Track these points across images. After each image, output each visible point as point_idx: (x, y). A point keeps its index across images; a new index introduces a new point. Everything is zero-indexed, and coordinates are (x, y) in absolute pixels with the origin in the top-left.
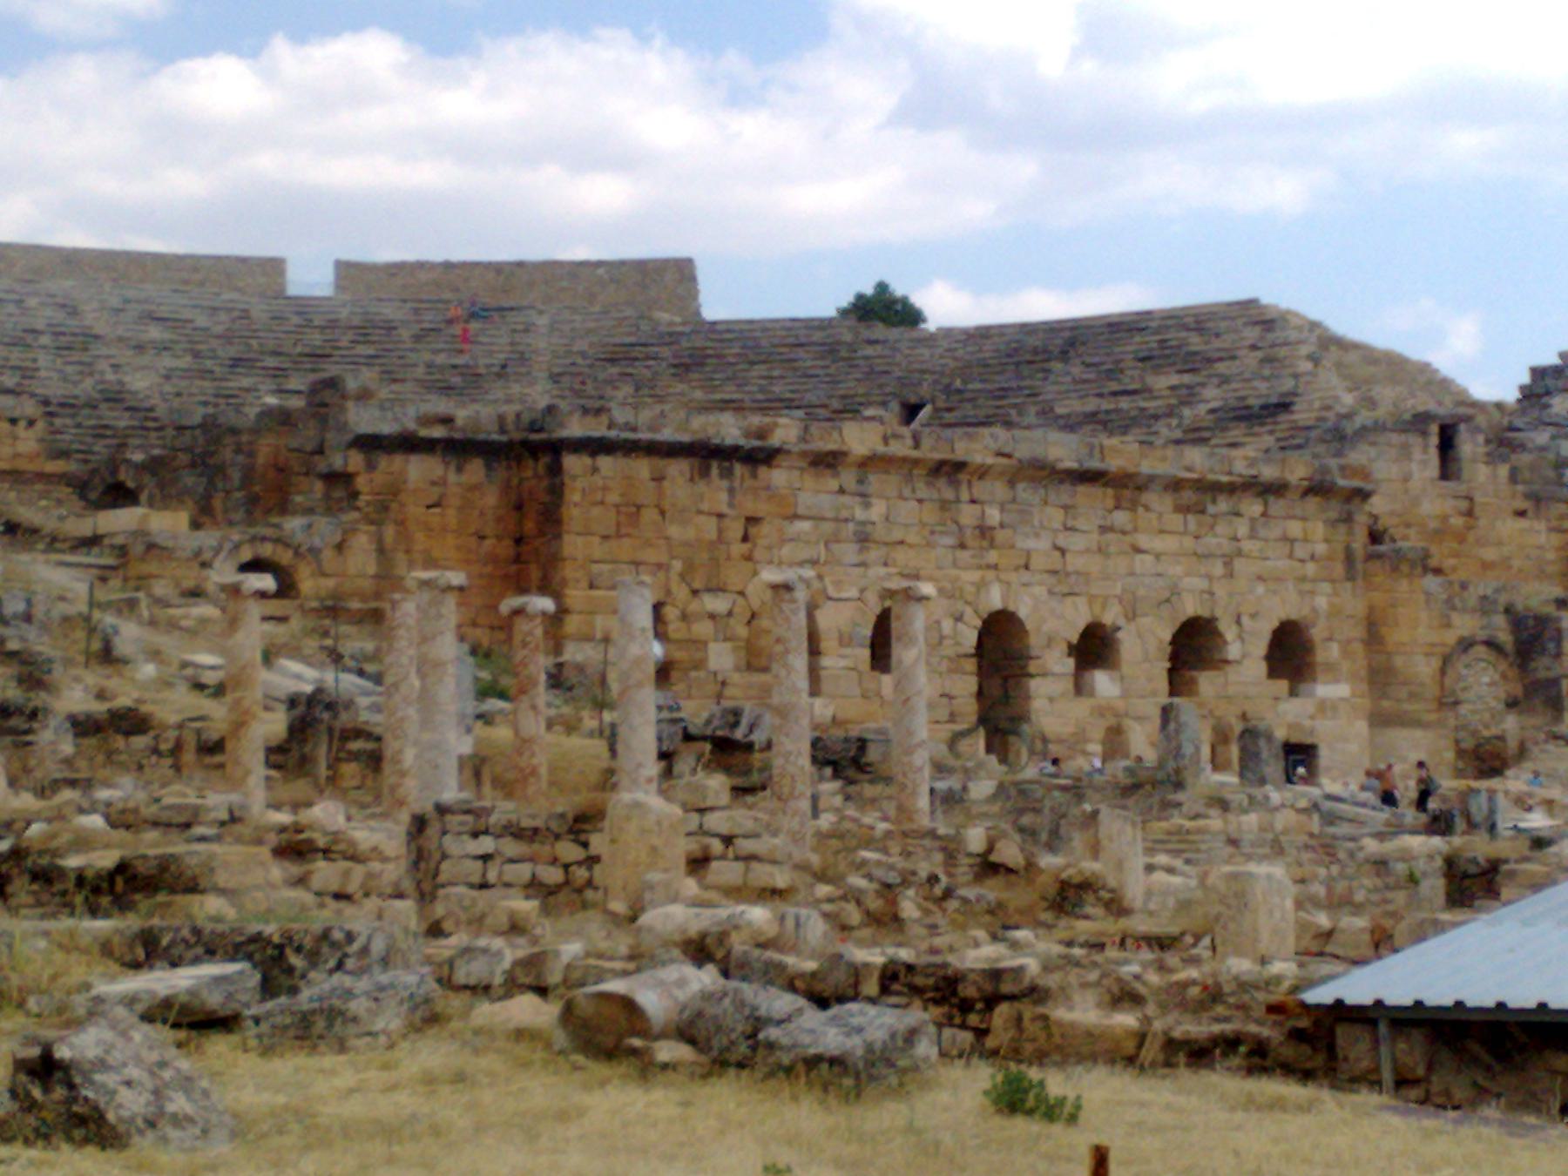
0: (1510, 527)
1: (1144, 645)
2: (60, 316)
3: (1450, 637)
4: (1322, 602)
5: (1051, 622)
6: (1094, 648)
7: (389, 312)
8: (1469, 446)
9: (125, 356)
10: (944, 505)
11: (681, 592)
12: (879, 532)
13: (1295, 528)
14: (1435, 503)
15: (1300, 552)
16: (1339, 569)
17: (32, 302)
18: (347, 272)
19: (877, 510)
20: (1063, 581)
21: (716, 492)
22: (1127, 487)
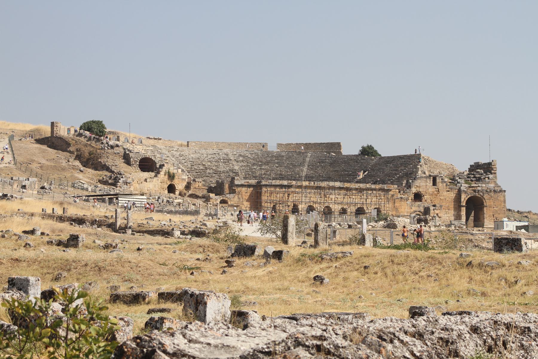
0: (445, 193)
2: (225, 156)
3: (412, 210)
6: (343, 212)
7: (283, 154)
8: (438, 180)
9: (235, 163)
14: (432, 189)
17: (221, 154)
18: (279, 145)
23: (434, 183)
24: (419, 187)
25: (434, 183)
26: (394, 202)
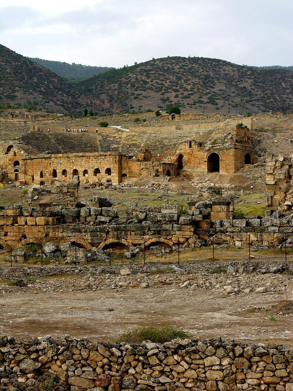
0: (197, 153)
1: (91, 171)
4: (112, 166)
5: (81, 170)
6: (85, 172)
10: (69, 160)
11: (44, 170)
13: (109, 159)
15: (109, 161)
16: (114, 163)
19: (62, 161)
20: (81, 166)
21: (47, 161)
22: (89, 157)
23: (190, 146)
24: (181, 149)
25: (190, 146)
26: (128, 163)
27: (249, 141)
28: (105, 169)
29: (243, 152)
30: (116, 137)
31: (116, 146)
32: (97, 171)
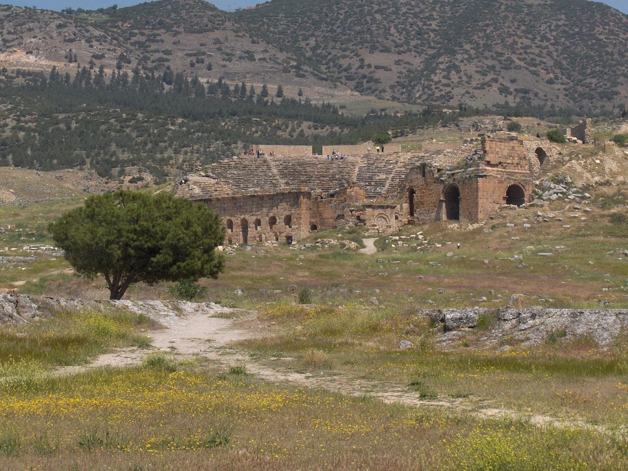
5: (251, 219)
6: (258, 223)
12: (226, 209)
13: (288, 200)
19: (226, 205)
27: (523, 162)
28: (283, 217)
29: (501, 182)
30: (391, 162)
31: (383, 176)
32: (273, 221)
